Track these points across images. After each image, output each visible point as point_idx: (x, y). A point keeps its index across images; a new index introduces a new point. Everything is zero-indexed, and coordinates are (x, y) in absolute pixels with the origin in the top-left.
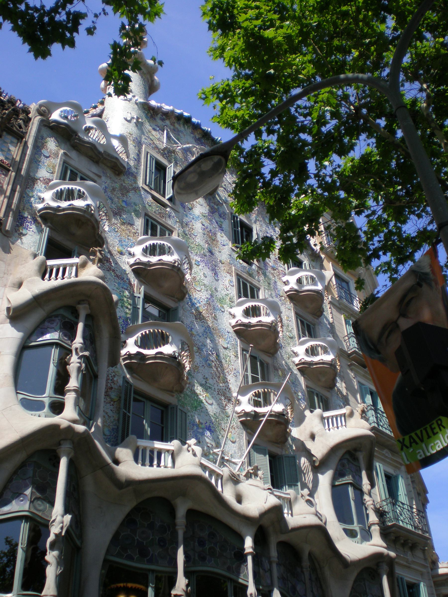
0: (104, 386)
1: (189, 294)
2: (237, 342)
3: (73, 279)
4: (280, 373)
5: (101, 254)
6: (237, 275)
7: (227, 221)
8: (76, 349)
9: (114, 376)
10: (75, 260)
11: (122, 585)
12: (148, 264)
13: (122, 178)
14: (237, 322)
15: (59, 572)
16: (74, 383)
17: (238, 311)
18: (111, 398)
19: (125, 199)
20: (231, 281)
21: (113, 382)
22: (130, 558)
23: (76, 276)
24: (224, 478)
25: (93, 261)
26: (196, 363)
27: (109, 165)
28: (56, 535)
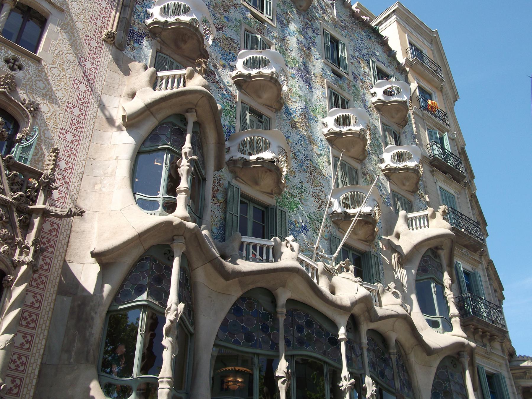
0: (211, 189)
1: (285, 104)
2: (329, 149)
6: (329, 87)
9: (220, 180)
11: (230, 368)
12: (249, 76)
14: (329, 131)
17: (330, 121)
18: (217, 199)
19: (226, 15)
20: (324, 93)
22: (237, 342)
24: (319, 272)
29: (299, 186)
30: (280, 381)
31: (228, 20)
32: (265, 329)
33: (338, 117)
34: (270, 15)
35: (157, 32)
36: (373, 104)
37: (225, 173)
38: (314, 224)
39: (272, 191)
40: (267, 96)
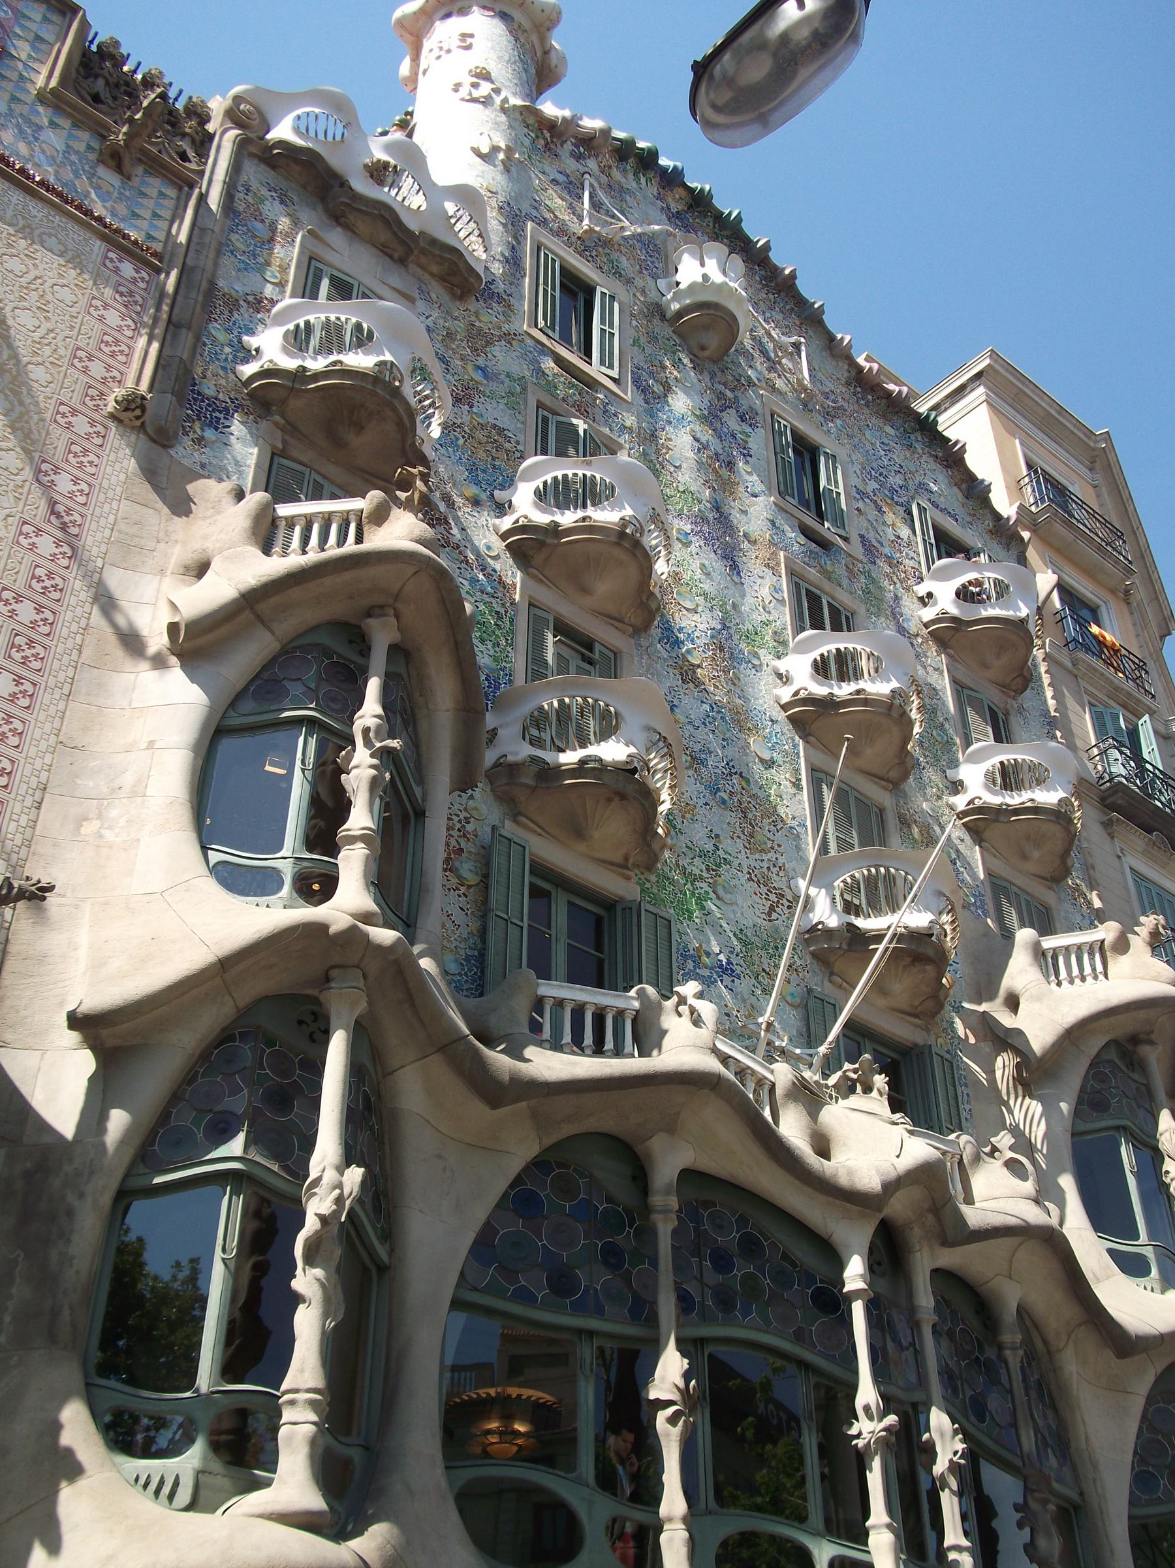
0: (442, 847)
1: (663, 616)
2: (795, 746)
3: (350, 547)
4: (916, 830)
5: (426, 483)
6: (792, 573)
7: (761, 431)
8: (366, 731)
10: (356, 504)
12: (554, 530)
13: (473, 305)
14: (796, 693)
15: (330, 1324)
16: (360, 819)
17: (799, 670)
18: (459, 877)
19: (481, 361)
20: (777, 589)
21: (464, 836)
22: (525, 1296)
23: (359, 540)
24: (779, 1091)
25: (407, 505)
26: (686, 795)
27: (435, 269)
28: (323, 1219)
29: (709, 847)
30: (662, 1416)
31: (486, 376)
32: (612, 1257)
33: (822, 655)
34: (611, 367)
35: (271, 398)
36: (926, 625)
37: (481, 799)
38: (756, 958)
39: (626, 859)
40: (607, 587)
